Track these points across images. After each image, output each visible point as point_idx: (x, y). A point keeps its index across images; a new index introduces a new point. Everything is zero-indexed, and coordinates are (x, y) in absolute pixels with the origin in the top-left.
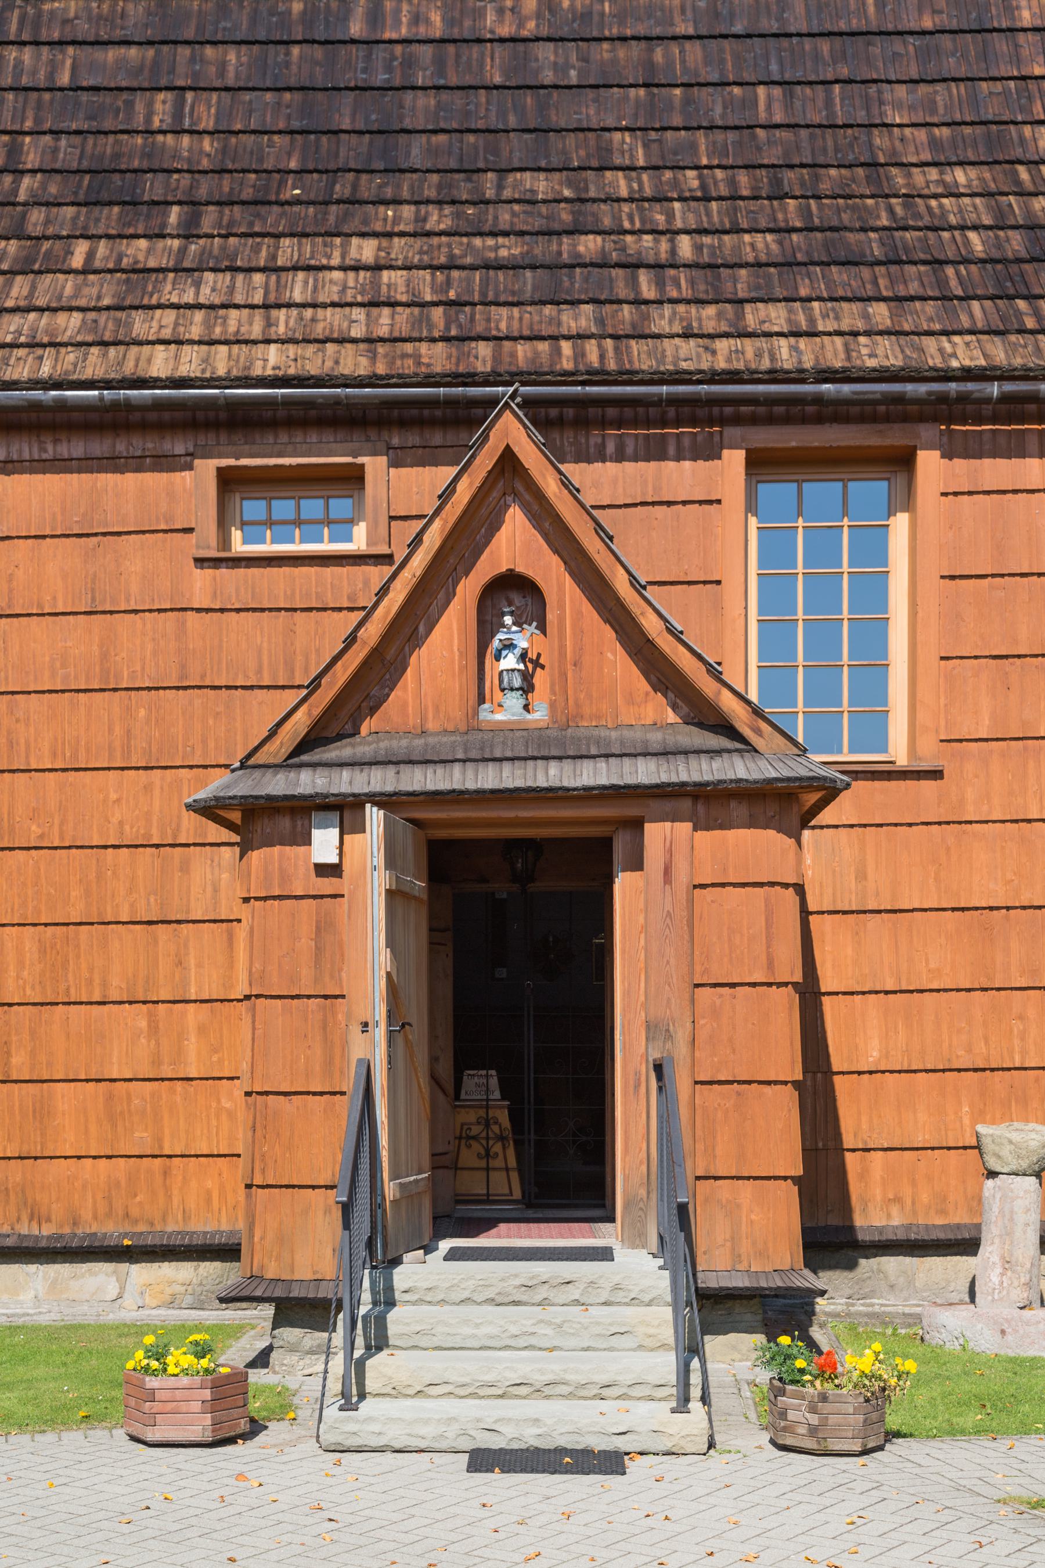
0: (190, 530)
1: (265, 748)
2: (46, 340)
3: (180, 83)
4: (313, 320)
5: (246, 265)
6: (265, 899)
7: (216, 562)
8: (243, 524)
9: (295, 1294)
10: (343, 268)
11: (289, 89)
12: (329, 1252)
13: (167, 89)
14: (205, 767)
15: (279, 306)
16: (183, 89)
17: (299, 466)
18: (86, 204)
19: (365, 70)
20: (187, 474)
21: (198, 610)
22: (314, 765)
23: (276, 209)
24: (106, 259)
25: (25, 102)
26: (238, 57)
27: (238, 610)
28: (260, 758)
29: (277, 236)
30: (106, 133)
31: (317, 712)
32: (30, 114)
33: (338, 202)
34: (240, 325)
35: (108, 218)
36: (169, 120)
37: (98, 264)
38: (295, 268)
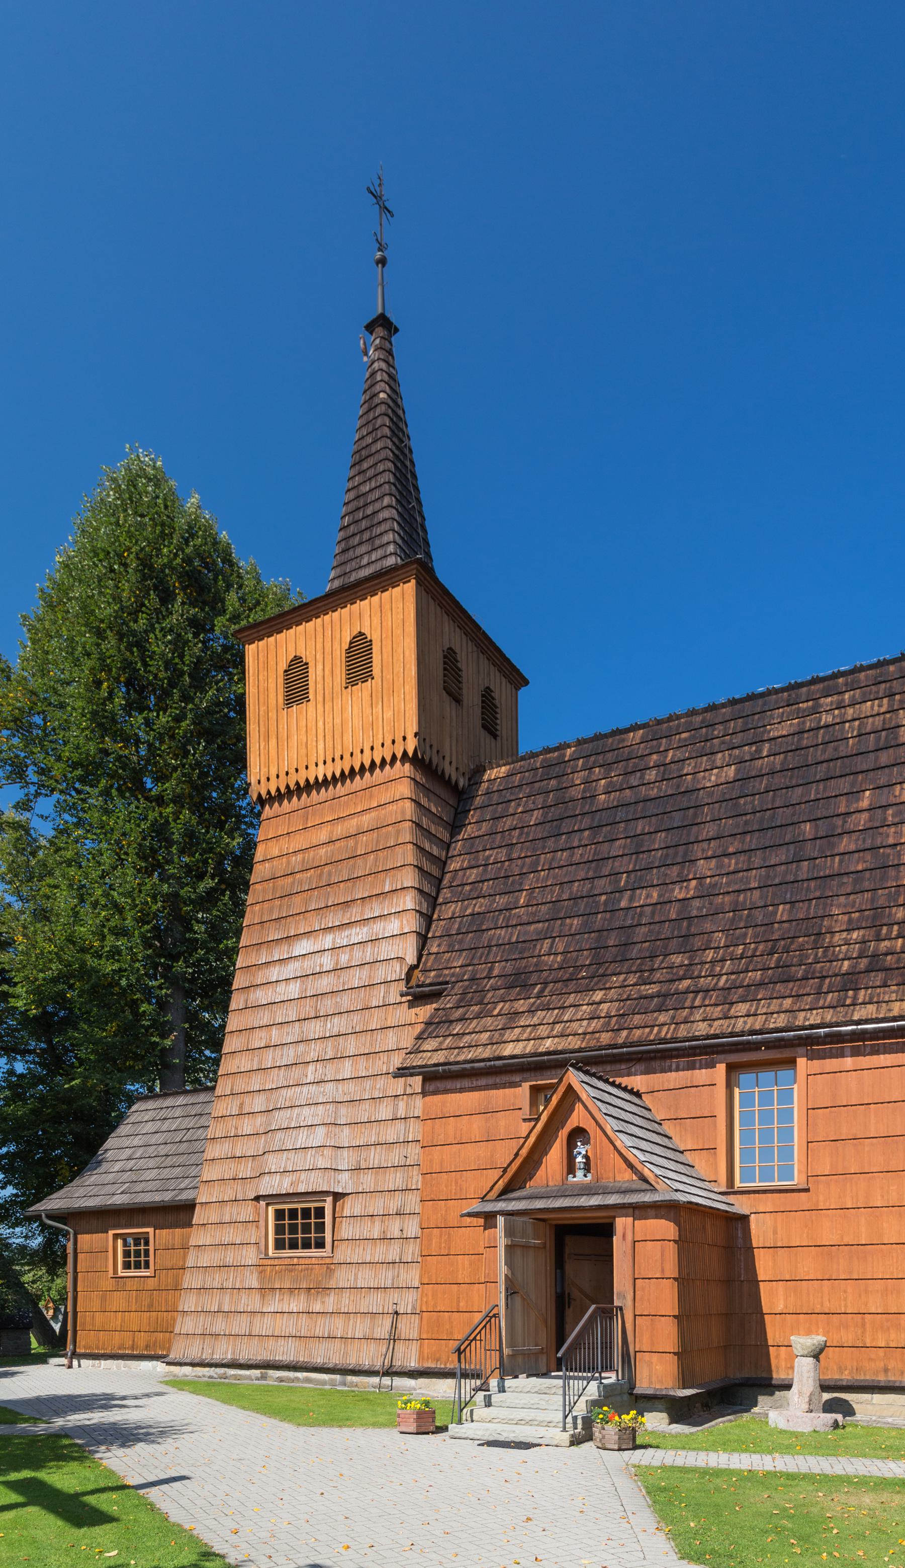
3: (554, 935)
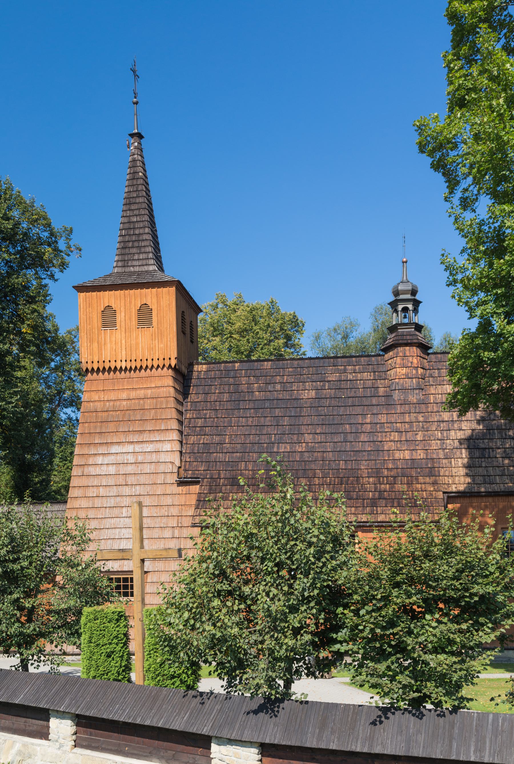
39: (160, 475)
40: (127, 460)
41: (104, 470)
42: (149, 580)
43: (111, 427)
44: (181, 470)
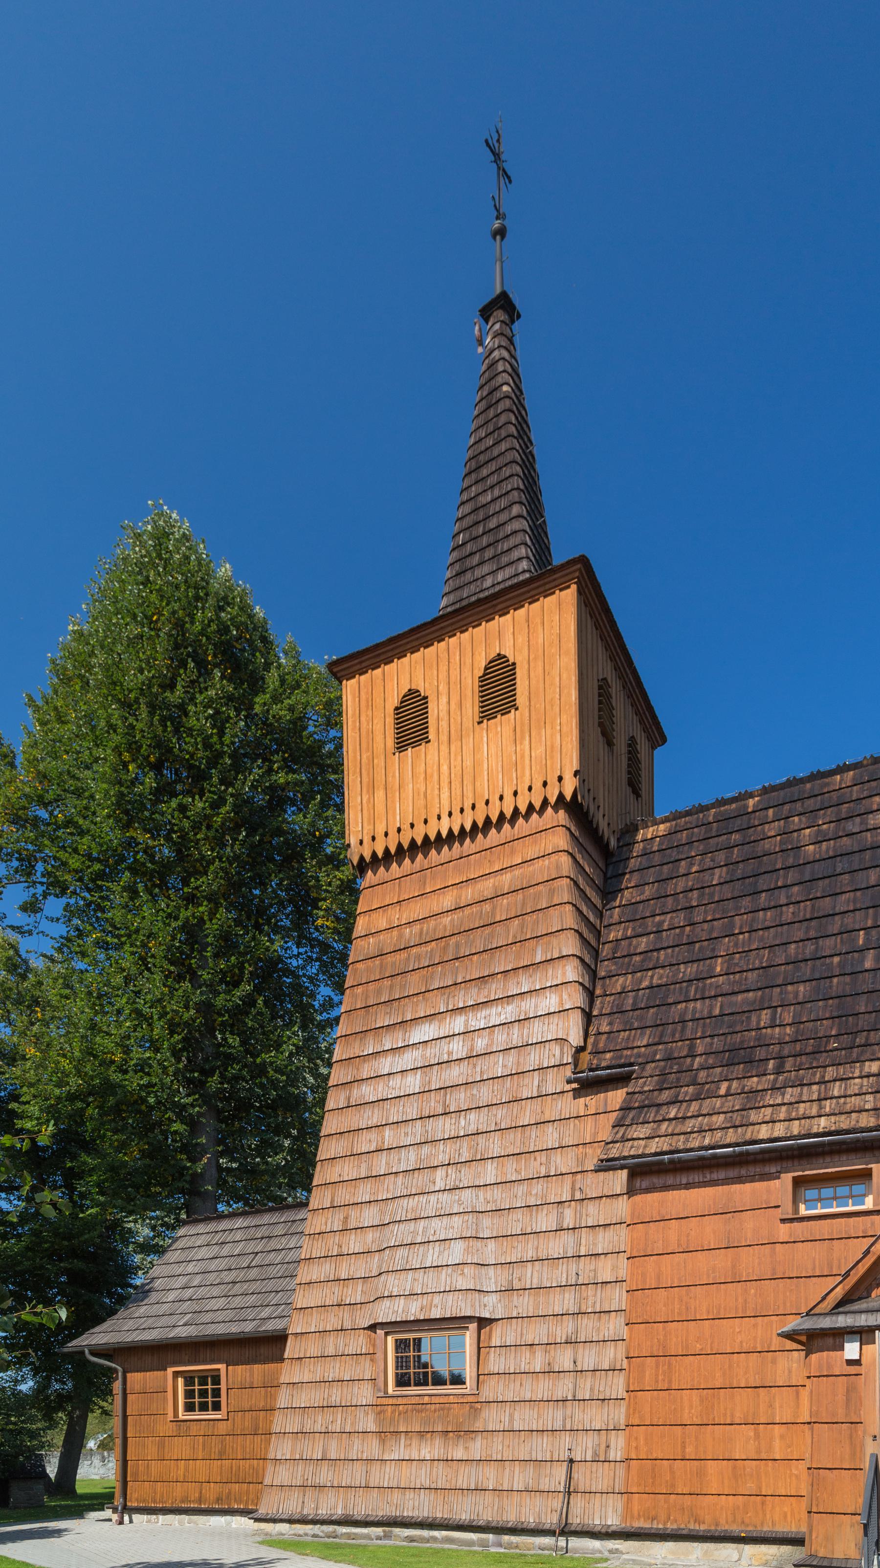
0: (778, 1207)
1: (819, 1306)
2: (707, 1128)
3: (775, 1004)
4: (845, 1103)
5: (808, 1082)
6: (819, 1377)
7: (791, 1220)
8: (806, 1201)
9: (834, 1565)
10: (861, 1077)
11: (832, 998)
12: (853, 1545)
13: (768, 1008)
14: (785, 1315)
15: (826, 1099)
16: (776, 1007)
17: (836, 1172)
18: (727, 1066)
19: (873, 983)
20: (777, 1181)
21: (782, 1243)
22: (846, 1313)
23: (824, 1054)
24: (737, 1089)
25: (697, 1025)
26: (805, 988)
27: (803, 1242)
28: (817, 1310)
29: (825, 1067)
30: (737, 1033)
31: (848, 1287)
32: (700, 1030)
33: (858, 1047)
34: (805, 1109)
35: (738, 1070)
36: (769, 1022)
37: (732, 1091)
38: (835, 1080)
39: (527, 1079)
40: (450, 1053)
41: (397, 1086)
42: (496, 1341)
43: (414, 983)
44: (585, 1057)
